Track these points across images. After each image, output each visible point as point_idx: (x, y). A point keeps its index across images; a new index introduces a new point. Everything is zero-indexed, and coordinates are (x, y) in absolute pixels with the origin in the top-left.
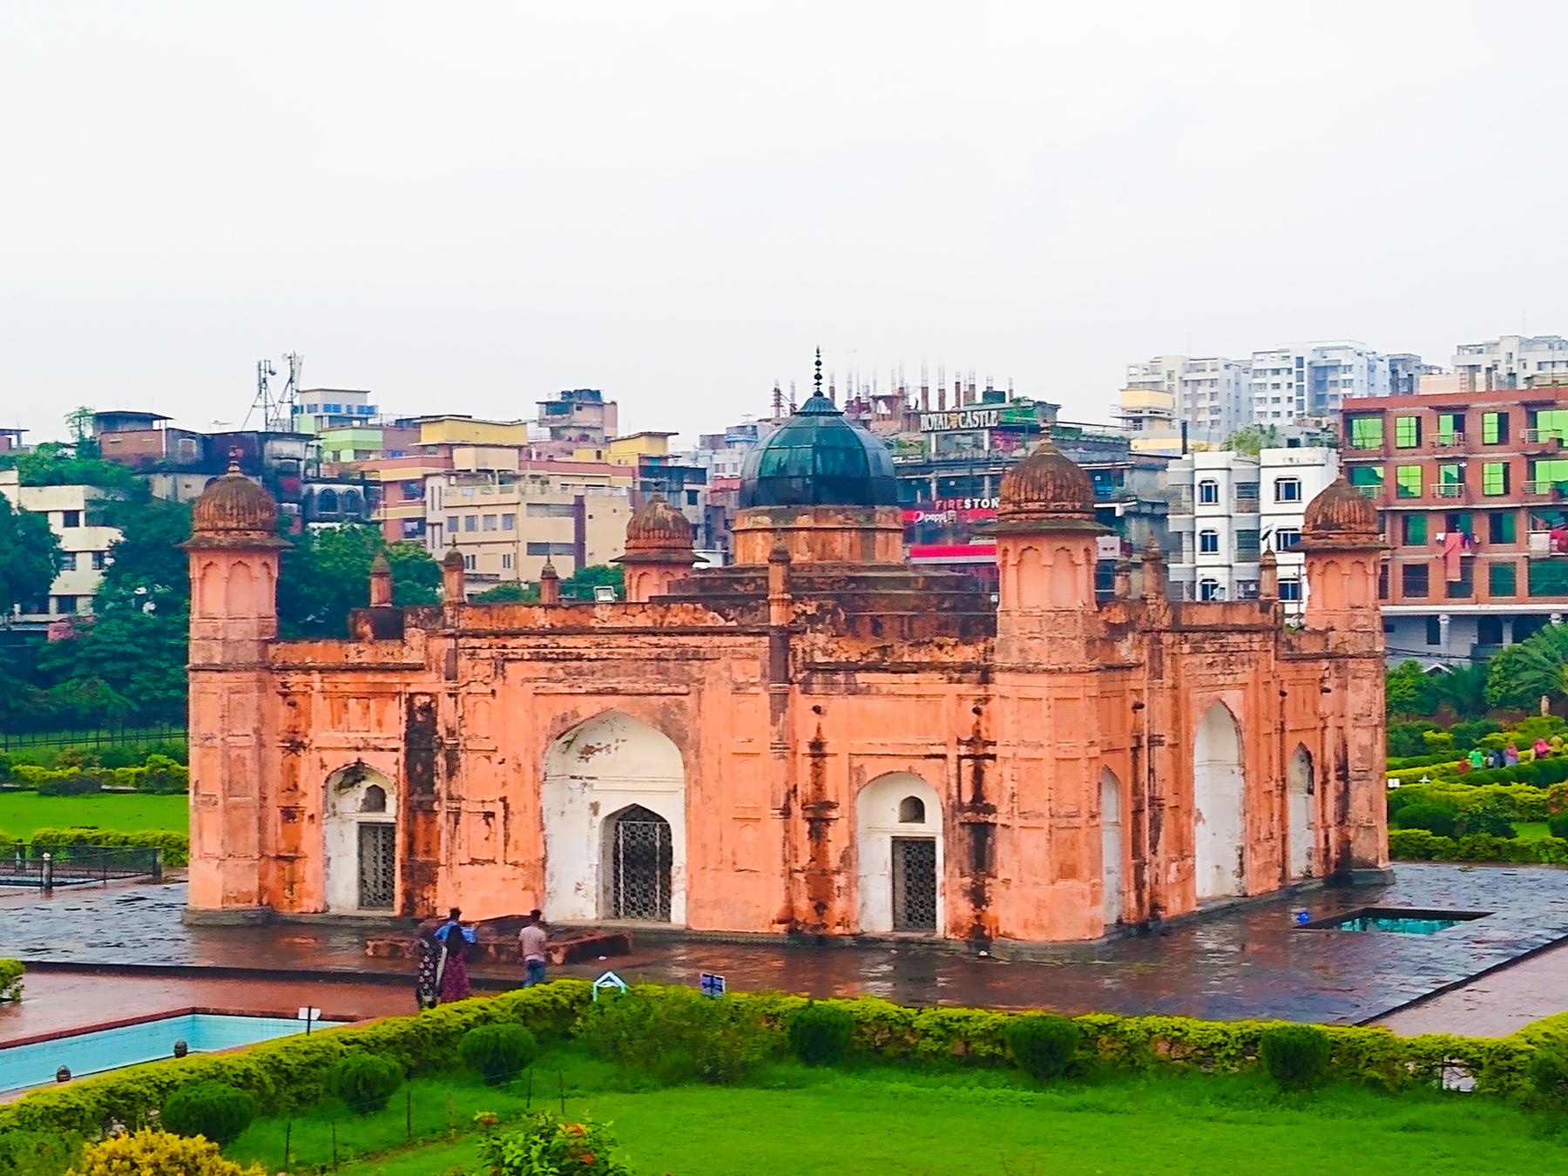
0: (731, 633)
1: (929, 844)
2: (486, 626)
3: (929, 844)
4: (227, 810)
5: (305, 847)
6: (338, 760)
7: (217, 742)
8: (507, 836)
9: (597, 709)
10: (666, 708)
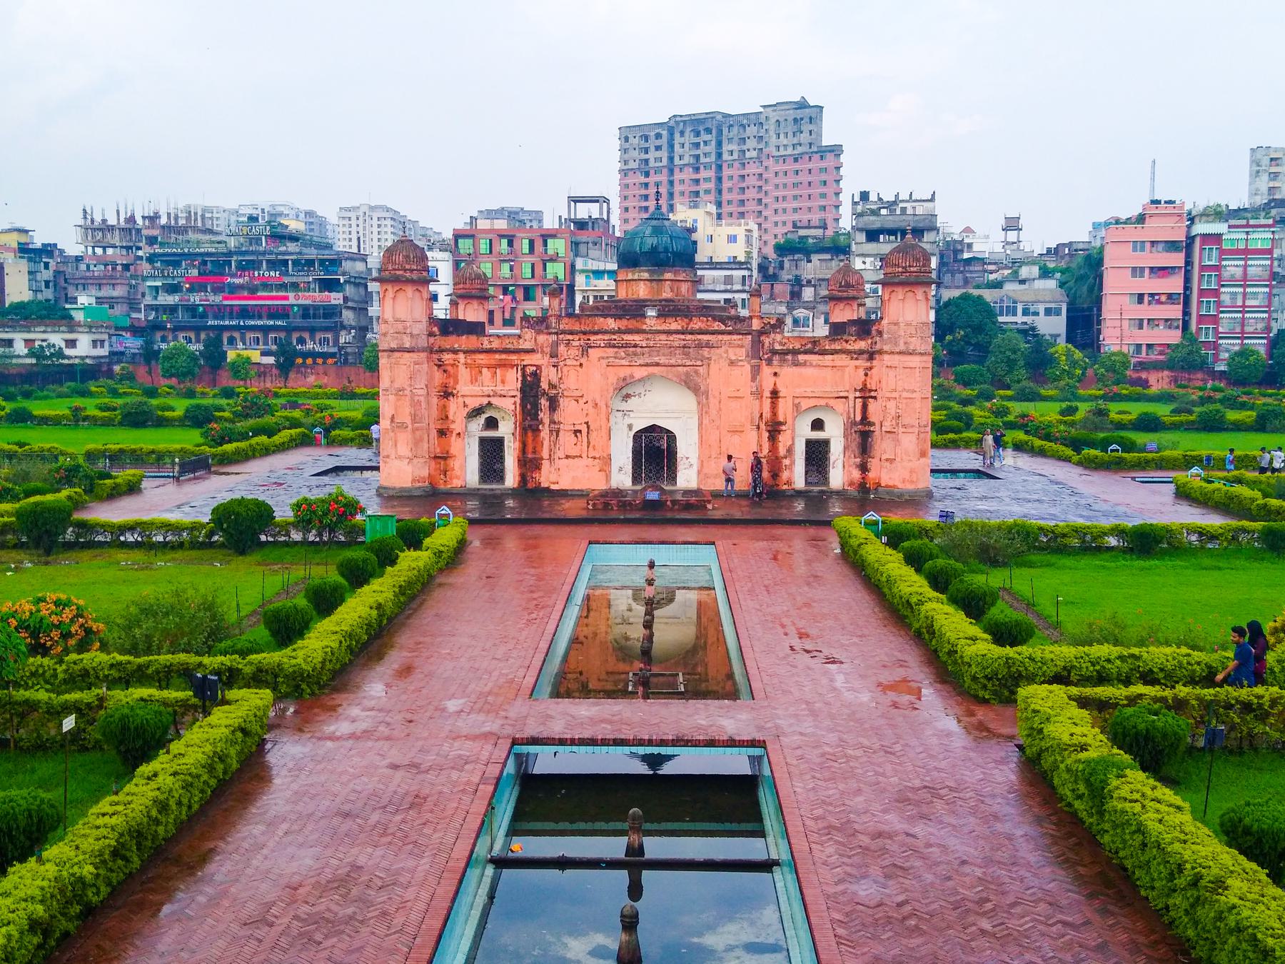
0: (730, 333)
1: (826, 443)
2: (577, 328)
3: (826, 443)
4: (414, 430)
5: (453, 451)
6: (474, 403)
7: (407, 392)
8: (589, 443)
9: (645, 374)
10: (687, 374)
